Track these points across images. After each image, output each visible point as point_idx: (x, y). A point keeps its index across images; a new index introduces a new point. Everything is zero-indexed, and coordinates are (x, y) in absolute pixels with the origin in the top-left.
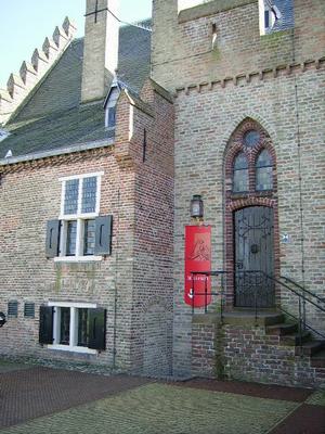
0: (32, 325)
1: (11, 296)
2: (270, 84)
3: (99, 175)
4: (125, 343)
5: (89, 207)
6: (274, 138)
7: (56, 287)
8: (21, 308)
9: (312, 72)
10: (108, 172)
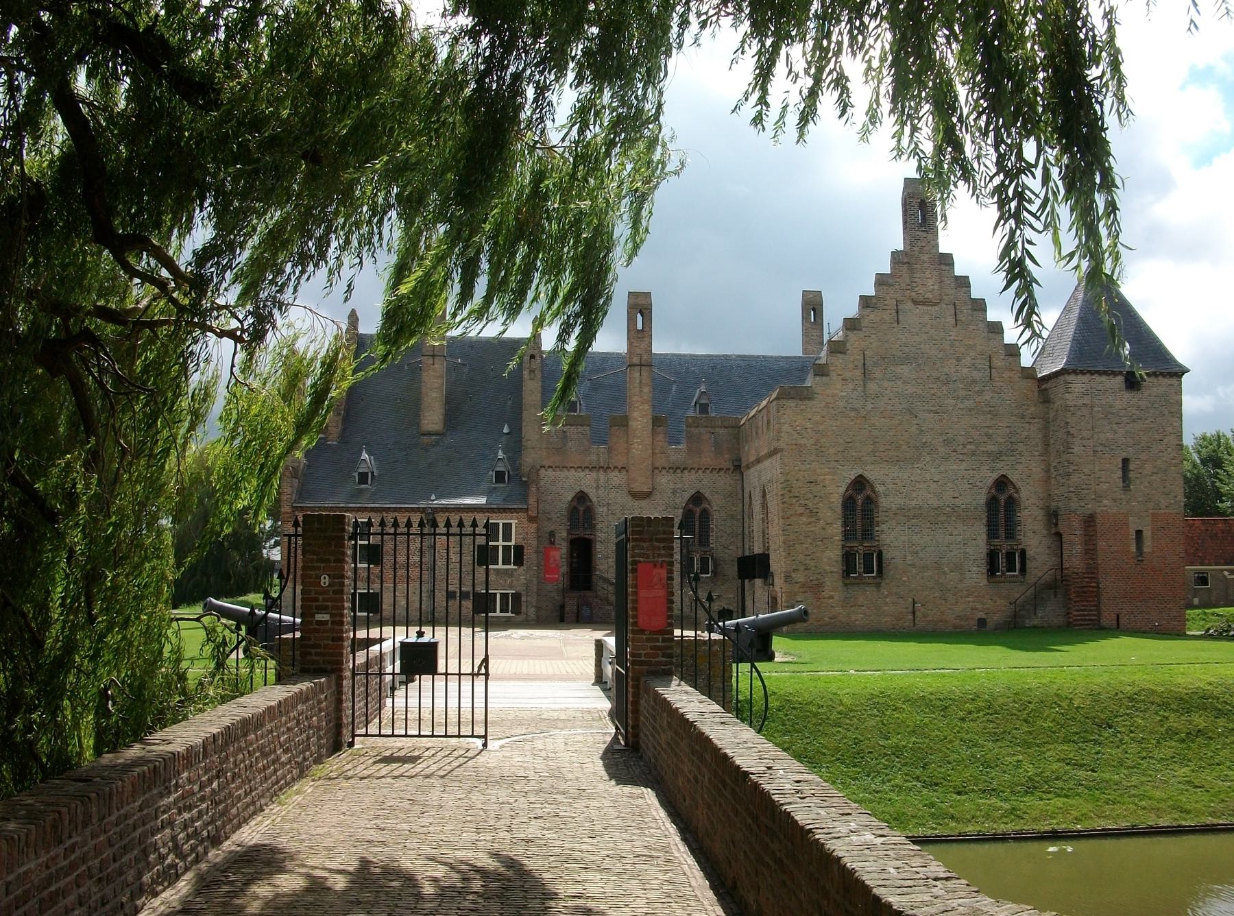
2: (594, 474)
3: (514, 522)
5: (507, 537)
6: (596, 504)
9: (616, 473)
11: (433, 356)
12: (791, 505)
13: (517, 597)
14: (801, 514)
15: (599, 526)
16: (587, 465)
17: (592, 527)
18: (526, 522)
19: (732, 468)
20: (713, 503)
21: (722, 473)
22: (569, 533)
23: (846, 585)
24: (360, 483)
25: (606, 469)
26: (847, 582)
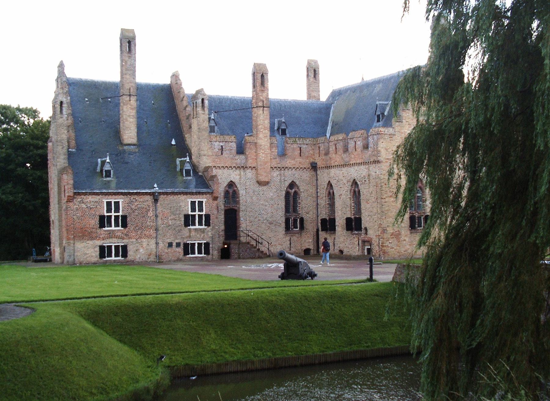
0: (180, 250)
1: (169, 241)
2: (238, 172)
3: (204, 200)
4: (216, 252)
5: (201, 210)
6: (239, 189)
7: (190, 237)
8: (174, 244)
9: (249, 170)
10: (208, 200)
11: (130, 95)
12: (386, 192)
13: (207, 245)
14: (391, 196)
15: (241, 202)
16: (234, 165)
17: (238, 202)
18: (211, 201)
19: (311, 168)
20: (300, 188)
21: (305, 170)
22: (225, 206)
23: (411, 233)
24: (107, 176)
25: (244, 168)
26: (413, 231)
